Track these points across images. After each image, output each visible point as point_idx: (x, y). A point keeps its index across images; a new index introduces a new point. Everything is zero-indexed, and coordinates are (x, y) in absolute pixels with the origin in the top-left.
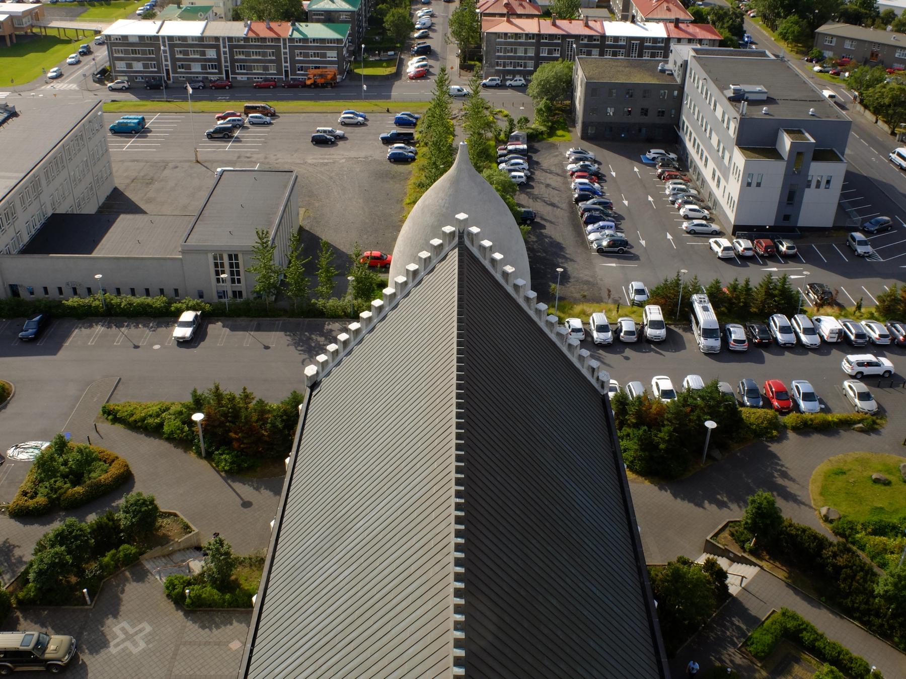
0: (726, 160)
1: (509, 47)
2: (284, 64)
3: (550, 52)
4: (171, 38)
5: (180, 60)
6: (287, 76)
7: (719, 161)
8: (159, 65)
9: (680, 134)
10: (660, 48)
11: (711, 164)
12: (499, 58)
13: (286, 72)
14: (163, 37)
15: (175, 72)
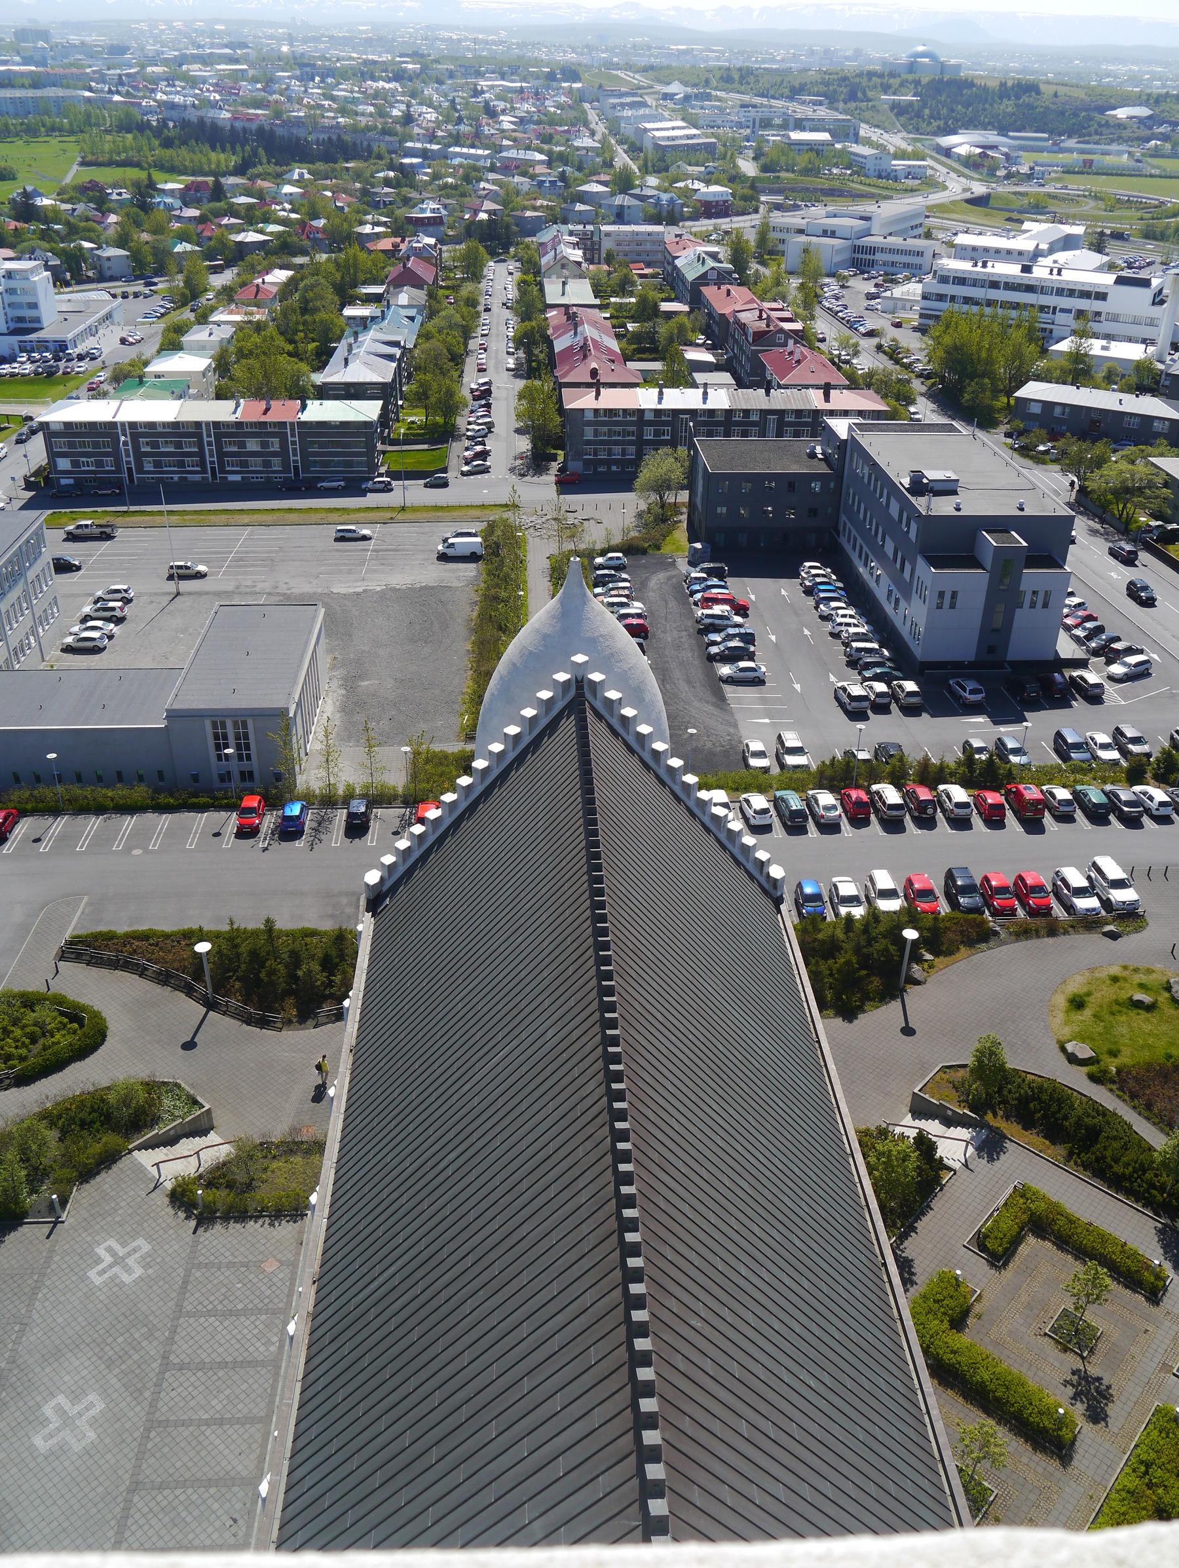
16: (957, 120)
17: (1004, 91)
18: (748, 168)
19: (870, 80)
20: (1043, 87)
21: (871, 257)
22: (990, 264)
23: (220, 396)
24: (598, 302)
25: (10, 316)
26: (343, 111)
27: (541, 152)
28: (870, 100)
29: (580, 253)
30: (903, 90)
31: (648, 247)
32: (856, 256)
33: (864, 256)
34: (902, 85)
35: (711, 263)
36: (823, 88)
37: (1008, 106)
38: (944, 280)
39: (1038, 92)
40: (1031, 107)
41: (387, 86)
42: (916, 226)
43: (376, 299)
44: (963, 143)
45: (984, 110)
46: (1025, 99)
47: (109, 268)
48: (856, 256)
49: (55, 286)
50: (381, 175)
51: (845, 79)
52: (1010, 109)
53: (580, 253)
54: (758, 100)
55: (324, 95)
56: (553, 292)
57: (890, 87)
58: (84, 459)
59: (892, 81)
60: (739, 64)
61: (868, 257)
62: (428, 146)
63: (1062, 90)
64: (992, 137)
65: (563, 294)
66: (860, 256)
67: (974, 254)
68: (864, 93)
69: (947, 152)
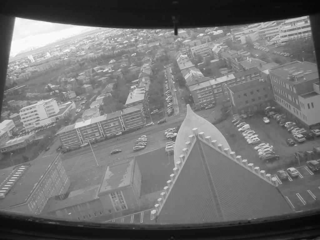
0: (297, 103)
1: (202, 94)
2: (122, 125)
3: (218, 91)
4: (80, 128)
5: (85, 135)
6: (125, 129)
7: (295, 105)
8: (78, 139)
9: (276, 102)
10: (258, 76)
11: (292, 107)
12: (200, 98)
13: (124, 128)
14: (77, 129)
15: (84, 140)
22: (296, 24)
23: (102, 114)
24: (194, 65)
25: (47, 110)
26: (121, 44)
29: (187, 56)
31: (204, 49)
38: (285, 31)
43: (137, 83)
47: (70, 96)
49: (58, 105)
50: (133, 55)
53: (187, 56)
55: (115, 42)
56: (181, 67)
58: (70, 141)
62: (143, 45)
65: (184, 66)
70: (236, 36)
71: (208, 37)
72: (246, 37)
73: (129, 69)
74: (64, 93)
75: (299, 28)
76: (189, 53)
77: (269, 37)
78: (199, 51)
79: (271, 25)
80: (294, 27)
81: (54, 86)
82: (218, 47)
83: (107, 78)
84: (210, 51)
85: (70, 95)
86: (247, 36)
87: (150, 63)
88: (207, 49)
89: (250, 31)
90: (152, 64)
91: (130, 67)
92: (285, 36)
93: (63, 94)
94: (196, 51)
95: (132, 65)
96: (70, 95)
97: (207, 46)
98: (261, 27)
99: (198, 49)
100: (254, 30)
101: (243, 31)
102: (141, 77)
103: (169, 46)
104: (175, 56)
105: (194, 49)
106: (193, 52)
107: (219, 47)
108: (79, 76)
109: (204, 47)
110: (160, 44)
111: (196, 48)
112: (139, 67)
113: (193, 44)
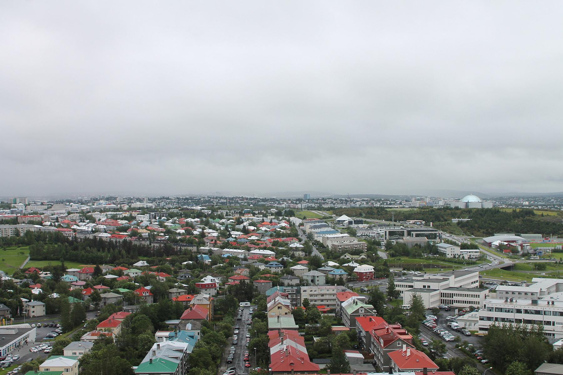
16: (493, 229)
17: (515, 215)
18: (383, 254)
19: (445, 211)
20: (535, 212)
21: (451, 299)
22: (514, 301)
27: (272, 250)
28: (446, 220)
30: (463, 215)
31: (327, 297)
32: (443, 298)
33: (447, 298)
34: (462, 213)
35: (360, 304)
36: (421, 216)
37: (517, 222)
38: (491, 309)
39: (534, 215)
40: (532, 221)
41: (193, 220)
42: (475, 282)
44: (497, 240)
45: (507, 223)
46: (527, 218)
47: (34, 312)
48: (443, 298)
51: (433, 211)
52: (520, 223)
53: (289, 301)
54: (388, 223)
57: (456, 214)
59: (457, 211)
60: (378, 205)
61: (449, 299)
63: (545, 213)
64: (512, 237)
66: (445, 298)
67: (507, 295)
68: (443, 217)
69: (490, 245)
70: (397, 289)
71: (343, 272)
72: (414, 296)
73: (171, 290)
74: (24, 300)
75: (519, 311)
76: (295, 297)
77: (460, 309)
78: (316, 298)
79: (468, 284)
80: (509, 306)
81: (7, 278)
82: (354, 302)
83: (120, 297)
84: (338, 305)
85: (32, 309)
86: (418, 294)
87: (213, 292)
88: (332, 297)
89: (424, 287)
90: (218, 293)
91: (172, 287)
92: (489, 319)
93: (21, 302)
94: (311, 295)
95: (176, 284)
96: (32, 309)
97: (335, 292)
98: (448, 284)
99: (315, 293)
100: (433, 286)
101: (412, 281)
102: (187, 320)
103: (262, 267)
104: (267, 293)
105: (306, 293)
106: (304, 296)
107: (357, 302)
108: (67, 273)
109: (328, 292)
110: (245, 256)
111: (311, 291)
112: (190, 296)
113: (310, 279)
